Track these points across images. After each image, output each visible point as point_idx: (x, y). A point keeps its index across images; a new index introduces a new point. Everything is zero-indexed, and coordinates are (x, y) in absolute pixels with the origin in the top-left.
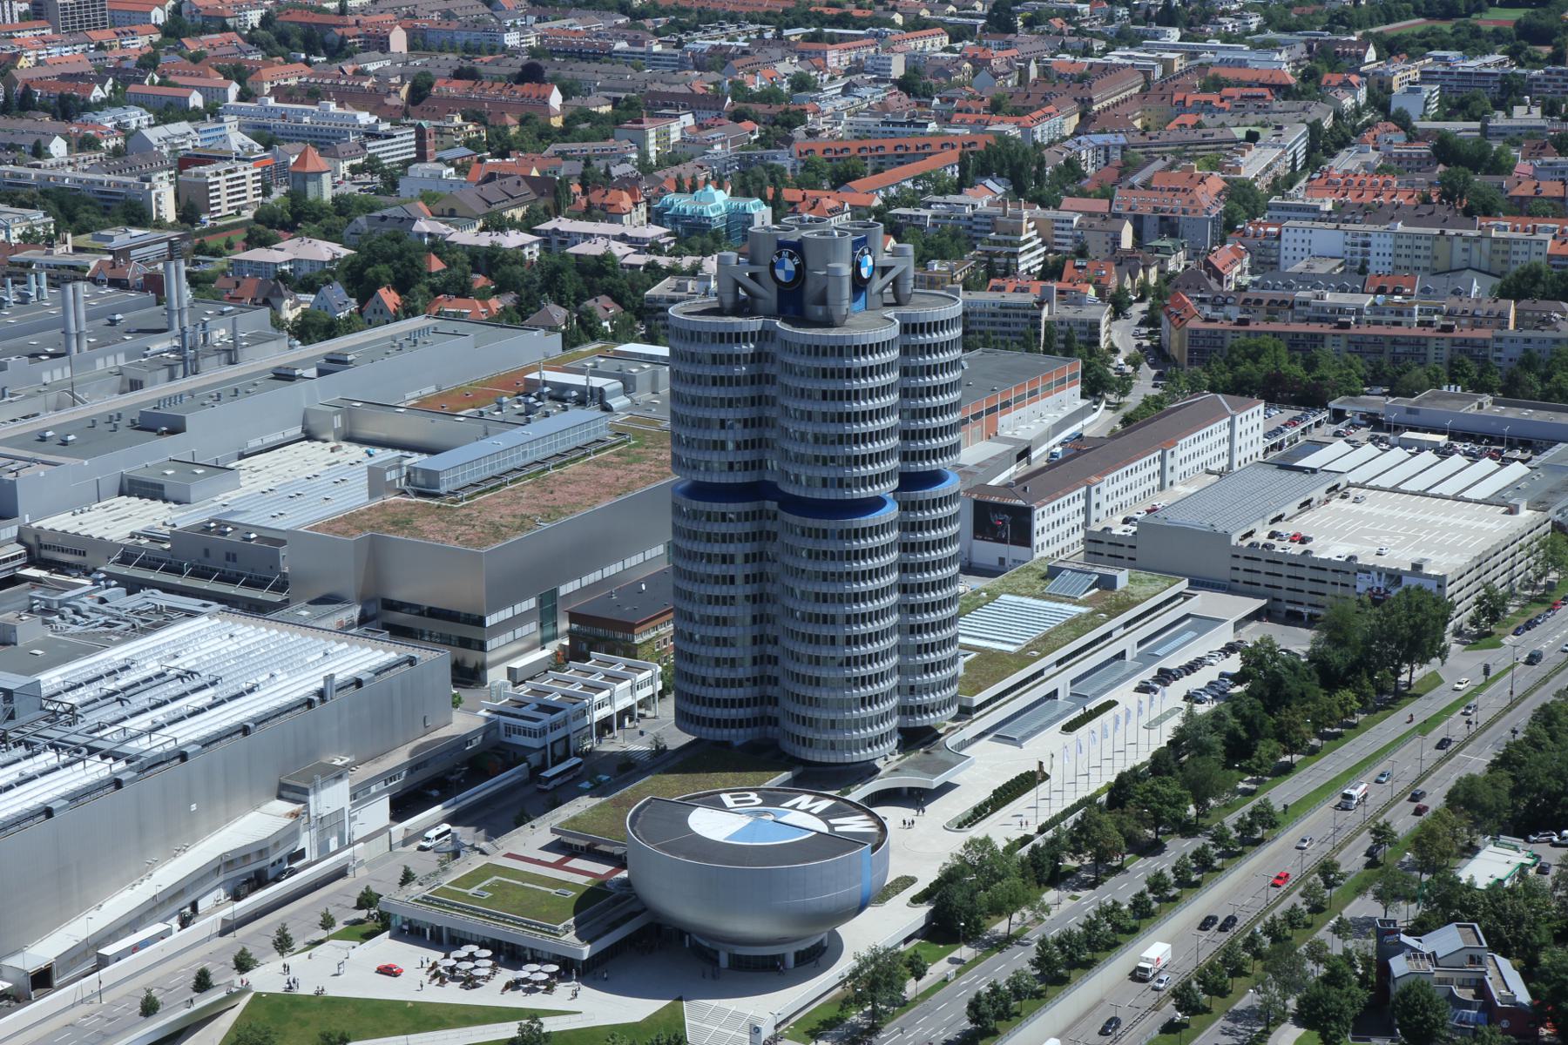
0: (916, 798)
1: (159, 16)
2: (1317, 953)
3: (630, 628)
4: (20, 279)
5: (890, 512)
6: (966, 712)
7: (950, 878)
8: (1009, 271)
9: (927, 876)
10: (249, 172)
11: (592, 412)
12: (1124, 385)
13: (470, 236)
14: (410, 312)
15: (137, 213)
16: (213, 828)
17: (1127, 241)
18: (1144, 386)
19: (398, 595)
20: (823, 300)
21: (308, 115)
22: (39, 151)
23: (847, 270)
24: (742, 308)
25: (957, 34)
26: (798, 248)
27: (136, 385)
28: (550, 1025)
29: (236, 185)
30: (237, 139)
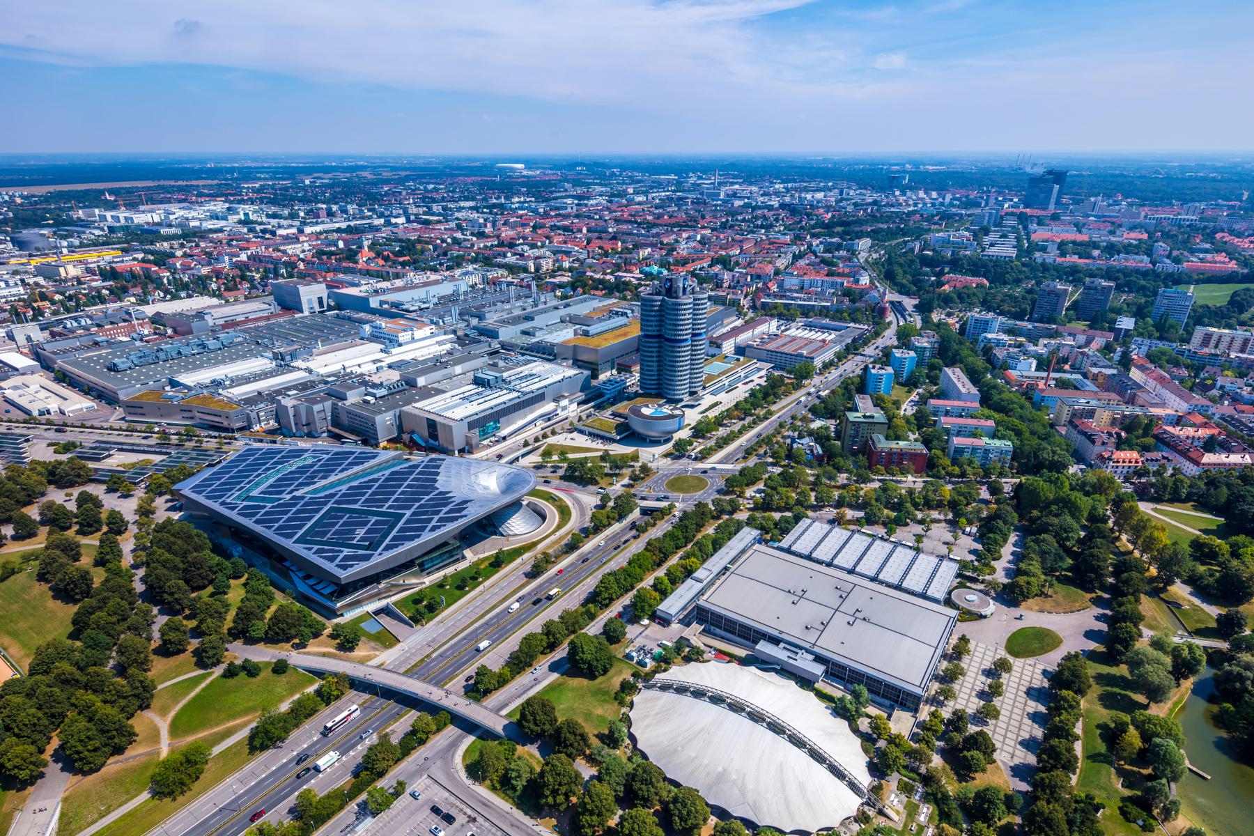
0: (692, 407)
1: (532, 224)
2: (777, 442)
3: (630, 367)
4: (500, 285)
5: (689, 343)
6: (704, 388)
7: (699, 423)
8: (721, 287)
9: (693, 424)
10: (550, 261)
11: (624, 318)
12: (745, 315)
13: (597, 276)
14: (584, 293)
15: (525, 270)
16: (539, 408)
17: (749, 279)
18: (751, 314)
19: (580, 358)
20: (676, 292)
21: (564, 248)
22: (505, 256)
23: (681, 285)
24: (658, 294)
25: (713, 230)
26: (671, 280)
27: (524, 309)
28: (611, 453)
29: (547, 264)
30: (548, 253)
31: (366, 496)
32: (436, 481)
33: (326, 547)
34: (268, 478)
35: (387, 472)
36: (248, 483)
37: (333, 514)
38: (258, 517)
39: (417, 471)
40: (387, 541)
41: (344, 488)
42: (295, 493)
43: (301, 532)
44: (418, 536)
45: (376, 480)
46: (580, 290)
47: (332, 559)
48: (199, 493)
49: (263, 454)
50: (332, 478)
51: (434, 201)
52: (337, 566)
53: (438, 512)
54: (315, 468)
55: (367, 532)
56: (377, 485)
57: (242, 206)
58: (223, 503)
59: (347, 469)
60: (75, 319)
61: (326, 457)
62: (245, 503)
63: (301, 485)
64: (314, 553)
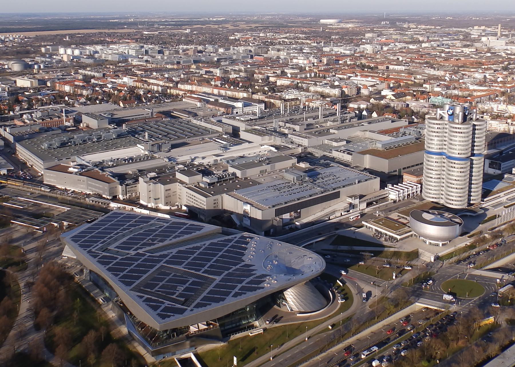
31: (189, 260)
32: (243, 254)
33: (153, 298)
34: (124, 236)
35: (208, 243)
36: (109, 238)
37: (162, 273)
38: (110, 265)
39: (231, 244)
40: (198, 300)
41: (174, 251)
42: (140, 251)
43: (138, 282)
44: (223, 300)
45: (198, 248)
46: (375, 115)
47: (155, 308)
48: (76, 241)
49: (124, 217)
50: (167, 242)
51: (272, 44)
52: (159, 315)
53: (241, 282)
54: (157, 233)
55: (186, 290)
56: (198, 252)
57: (145, 46)
58: (89, 252)
59: (179, 237)
60: (30, 114)
61: (166, 225)
62: (104, 254)
63: (145, 245)
64: (144, 301)
